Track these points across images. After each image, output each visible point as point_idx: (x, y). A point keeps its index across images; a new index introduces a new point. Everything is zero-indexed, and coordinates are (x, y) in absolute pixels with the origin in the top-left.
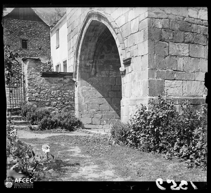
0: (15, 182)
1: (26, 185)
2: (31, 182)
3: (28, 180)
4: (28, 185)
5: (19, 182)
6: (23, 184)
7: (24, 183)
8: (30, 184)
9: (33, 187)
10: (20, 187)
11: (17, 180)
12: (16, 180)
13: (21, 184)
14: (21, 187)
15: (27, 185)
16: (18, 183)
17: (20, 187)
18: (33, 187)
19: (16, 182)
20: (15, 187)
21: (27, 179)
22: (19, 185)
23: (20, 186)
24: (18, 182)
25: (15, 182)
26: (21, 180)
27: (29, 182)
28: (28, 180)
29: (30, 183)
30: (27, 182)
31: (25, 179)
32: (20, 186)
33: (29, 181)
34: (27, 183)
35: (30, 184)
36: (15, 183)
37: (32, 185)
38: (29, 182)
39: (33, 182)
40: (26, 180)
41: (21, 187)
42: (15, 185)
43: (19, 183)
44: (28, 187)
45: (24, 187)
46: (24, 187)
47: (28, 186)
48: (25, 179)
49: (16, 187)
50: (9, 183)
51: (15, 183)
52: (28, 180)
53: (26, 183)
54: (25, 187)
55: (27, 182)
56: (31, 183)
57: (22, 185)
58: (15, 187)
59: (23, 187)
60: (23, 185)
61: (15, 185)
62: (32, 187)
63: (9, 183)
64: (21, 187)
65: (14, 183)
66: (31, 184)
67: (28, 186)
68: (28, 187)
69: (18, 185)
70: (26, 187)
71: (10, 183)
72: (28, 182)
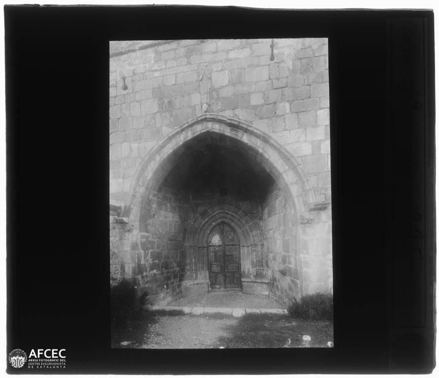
0: (30, 357)
1: (51, 362)
2: (62, 355)
3: (56, 353)
4: (56, 362)
5: (39, 357)
6: (46, 360)
7: (48, 359)
8: (59, 360)
9: (64, 367)
10: (39, 366)
11: (34, 353)
12: (33, 353)
13: (42, 360)
14: (41, 367)
15: (53, 362)
16: (36, 359)
17: (39, 366)
18: (64, 367)
19: (33, 357)
20: (31, 366)
21: (53, 350)
22: (38, 362)
23: (40, 364)
24: (36, 357)
25: (30, 357)
26: (42, 353)
27: (57, 357)
28: (55, 352)
29: (59, 358)
30: (53, 357)
31: (50, 350)
32: (40, 364)
33: (58, 355)
34: (54, 359)
35: (59, 360)
36: (30, 359)
37: (64, 362)
38: (57, 357)
39: (65, 357)
40: (51, 352)
41: (41, 367)
42: (30, 362)
43: (37, 358)
44: (56, 366)
45: (48, 367)
46: (48, 367)
47: (55, 364)
48: (50, 350)
49: (31, 367)
50: (18, 359)
51: (30, 359)
52: (55, 352)
53: (51, 358)
54: (49, 366)
55: (53, 357)
56: (62, 359)
57: (43, 362)
58: (31, 366)
59: (46, 366)
60: (45, 362)
61: (30, 362)
62: (63, 366)
63: (18, 359)
64: (43, 366)
65: (28, 359)
66: (61, 360)
67: (55, 364)
68: (56, 367)
69: (36, 362)
70: (52, 366)
71: (20, 358)
72: (55, 355)
